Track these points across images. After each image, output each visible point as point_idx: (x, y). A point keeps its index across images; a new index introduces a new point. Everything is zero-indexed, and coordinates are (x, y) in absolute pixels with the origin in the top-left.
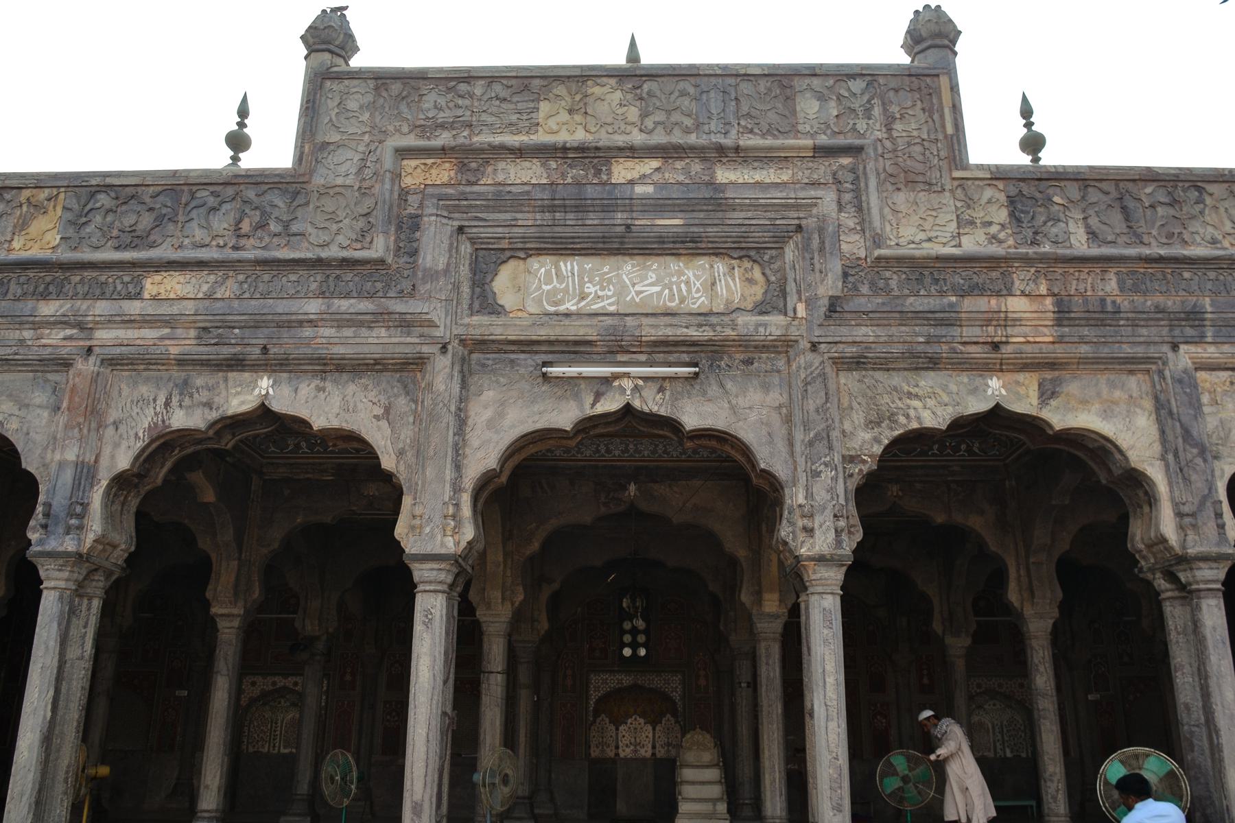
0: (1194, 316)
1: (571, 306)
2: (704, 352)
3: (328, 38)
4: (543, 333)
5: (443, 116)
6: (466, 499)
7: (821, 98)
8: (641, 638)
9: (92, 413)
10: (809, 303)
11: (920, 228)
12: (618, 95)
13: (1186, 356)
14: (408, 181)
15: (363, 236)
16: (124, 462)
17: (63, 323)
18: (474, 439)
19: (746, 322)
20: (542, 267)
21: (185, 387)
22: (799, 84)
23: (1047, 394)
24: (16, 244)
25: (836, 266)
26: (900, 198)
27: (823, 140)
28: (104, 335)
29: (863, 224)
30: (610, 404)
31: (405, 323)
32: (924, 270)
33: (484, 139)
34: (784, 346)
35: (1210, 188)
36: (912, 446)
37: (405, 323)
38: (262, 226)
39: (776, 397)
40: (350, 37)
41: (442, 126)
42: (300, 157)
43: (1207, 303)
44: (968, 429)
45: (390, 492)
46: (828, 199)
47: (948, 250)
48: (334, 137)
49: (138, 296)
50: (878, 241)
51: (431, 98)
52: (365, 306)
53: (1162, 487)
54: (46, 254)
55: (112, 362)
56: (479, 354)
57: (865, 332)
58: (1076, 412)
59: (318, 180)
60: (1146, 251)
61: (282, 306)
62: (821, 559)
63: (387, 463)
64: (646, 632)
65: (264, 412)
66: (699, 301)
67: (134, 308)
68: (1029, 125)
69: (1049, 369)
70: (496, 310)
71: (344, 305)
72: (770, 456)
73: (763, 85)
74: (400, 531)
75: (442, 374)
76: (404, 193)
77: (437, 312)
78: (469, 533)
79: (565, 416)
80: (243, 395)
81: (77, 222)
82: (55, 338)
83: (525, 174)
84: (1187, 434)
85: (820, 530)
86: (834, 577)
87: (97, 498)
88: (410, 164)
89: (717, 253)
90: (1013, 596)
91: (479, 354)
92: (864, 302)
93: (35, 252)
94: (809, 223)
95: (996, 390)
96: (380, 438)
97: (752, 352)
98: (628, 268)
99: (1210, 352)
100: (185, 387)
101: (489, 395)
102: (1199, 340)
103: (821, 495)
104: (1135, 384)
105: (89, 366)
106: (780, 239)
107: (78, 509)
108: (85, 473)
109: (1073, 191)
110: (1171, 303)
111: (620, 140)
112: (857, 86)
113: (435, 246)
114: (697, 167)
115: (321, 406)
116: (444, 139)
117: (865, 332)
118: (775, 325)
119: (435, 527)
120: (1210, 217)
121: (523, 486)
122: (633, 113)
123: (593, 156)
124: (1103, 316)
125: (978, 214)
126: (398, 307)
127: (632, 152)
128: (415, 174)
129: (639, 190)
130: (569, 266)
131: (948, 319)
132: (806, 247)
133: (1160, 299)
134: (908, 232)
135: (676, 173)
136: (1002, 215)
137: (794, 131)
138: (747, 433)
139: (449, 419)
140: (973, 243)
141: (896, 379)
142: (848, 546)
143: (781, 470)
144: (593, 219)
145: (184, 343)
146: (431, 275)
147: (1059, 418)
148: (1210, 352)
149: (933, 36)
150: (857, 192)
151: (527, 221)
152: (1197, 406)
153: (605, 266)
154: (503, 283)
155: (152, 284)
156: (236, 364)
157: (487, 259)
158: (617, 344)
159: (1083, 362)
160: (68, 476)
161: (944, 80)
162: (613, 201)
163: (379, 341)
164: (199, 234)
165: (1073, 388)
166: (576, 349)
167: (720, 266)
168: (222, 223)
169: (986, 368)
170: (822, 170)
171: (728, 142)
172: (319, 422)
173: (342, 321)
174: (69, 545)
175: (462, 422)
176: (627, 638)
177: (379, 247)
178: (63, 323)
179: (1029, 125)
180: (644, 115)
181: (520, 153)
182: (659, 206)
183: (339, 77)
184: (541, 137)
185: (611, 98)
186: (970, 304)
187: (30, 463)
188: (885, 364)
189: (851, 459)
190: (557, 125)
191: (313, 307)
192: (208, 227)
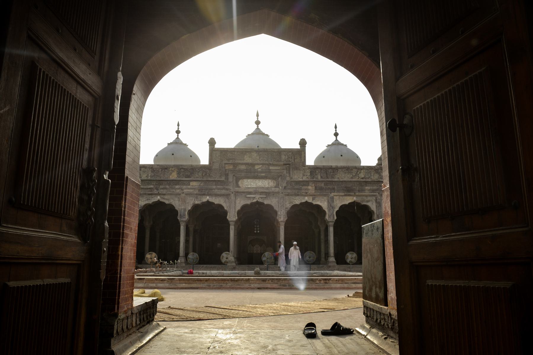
0: (334, 189)
2: (268, 194)
3: (212, 142)
4: (246, 191)
9: (184, 201)
11: (298, 176)
13: (332, 194)
15: (220, 177)
16: (190, 208)
17: (179, 189)
18: (237, 205)
19: (273, 189)
20: (245, 180)
21: (197, 198)
23: (313, 199)
26: (295, 171)
27: (285, 163)
28: (185, 191)
31: (227, 189)
32: (298, 183)
33: (237, 161)
34: (278, 193)
35: (340, 170)
37: (227, 189)
38: (206, 175)
39: (277, 200)
41: (231, 159)
43: (336, 187)
44: (302, 204)
45: (226, 213)
46: (285, 172)
47: (301, 180)
49: (189, 185)
50: (291, 178)
52: (221, 187)
53: (327, 212)
55: (186, 194)
56: (237, 193)
57: (289, 191)
59: (213, 168)
60: (328, 180)
61: (210, 187)
62: (281, 221)
63: (225, 208)
65: (208, 201)
66: (267, 186)
67: (189, 187)
69: (314, 197)
70: (239, 187)
71: (219, 187)
72: (276, 208)
74: (228, 217)
75: (232, 195)
76: (226, 170)
77: (231, 188)
78: (237, 218)
79: (249, 202)
80: (206, 199)
81: (179, 173)
82: (178, 191)
83: (243, 167)
85: (282, 217)
86: (283, 224)
87: (186, 213)
89: (270, 179)
91: (237, 193)
92: (288, 187)
95: (306, 199)
96: (224, 205)
97: (274, 194)
98: (257, 181)
99: (336, 194)
100: (197, 198)
102: (334, 192)
103: (282, 213)
104: (325, 198)
105: (184, 195)
106: (279, 177)
107: (184, 215)
108: (185, 210)
111: (256, 162)
112: (290, 153)
113: (231, 179)
115: (216, 201)
116: (230, 162)
119: (232, 217)
120: (338, 174)
121: (244, 211)
122: (258, 157)
123: (253, 165)
124: (321, 189)
125: (306, 174)
128: (228, 167)
130: (249, 180)
132: (282, 179)
136: (309, 174)
138: (273, 205)
140: (305, 178)
142: (285, 219)
143: (277, 210)
145: (197, 192)
147: (315, 203)
149: (303, 143)
150: (289, 170)
152: (333, 201)
154: (240, 183)
155: (191, 183)
156: (204, 195)
157: (237, 180)
158: (256, 193)
159: (318, 195)
160: (183, 211)
163: (223, 192)
164: (197, 176)
165: (317, 199)
166: (250, 193)
167: (270, 181)
168: (200, 174)
169: (305, 196)
170: (285, 167)
172: (216, 203)
173: (218, 189)
174: (184, 220)
176: (255, 229)
177: (223, 179)
178: (179, 189)
180: (260, 158)
181: (242, 164)
184: (245, 161)
185: (255, 155)
186: (303, 187)
187: (177, 208)
188: (292, 195)
190: (248, 159)
191: (214, 187)
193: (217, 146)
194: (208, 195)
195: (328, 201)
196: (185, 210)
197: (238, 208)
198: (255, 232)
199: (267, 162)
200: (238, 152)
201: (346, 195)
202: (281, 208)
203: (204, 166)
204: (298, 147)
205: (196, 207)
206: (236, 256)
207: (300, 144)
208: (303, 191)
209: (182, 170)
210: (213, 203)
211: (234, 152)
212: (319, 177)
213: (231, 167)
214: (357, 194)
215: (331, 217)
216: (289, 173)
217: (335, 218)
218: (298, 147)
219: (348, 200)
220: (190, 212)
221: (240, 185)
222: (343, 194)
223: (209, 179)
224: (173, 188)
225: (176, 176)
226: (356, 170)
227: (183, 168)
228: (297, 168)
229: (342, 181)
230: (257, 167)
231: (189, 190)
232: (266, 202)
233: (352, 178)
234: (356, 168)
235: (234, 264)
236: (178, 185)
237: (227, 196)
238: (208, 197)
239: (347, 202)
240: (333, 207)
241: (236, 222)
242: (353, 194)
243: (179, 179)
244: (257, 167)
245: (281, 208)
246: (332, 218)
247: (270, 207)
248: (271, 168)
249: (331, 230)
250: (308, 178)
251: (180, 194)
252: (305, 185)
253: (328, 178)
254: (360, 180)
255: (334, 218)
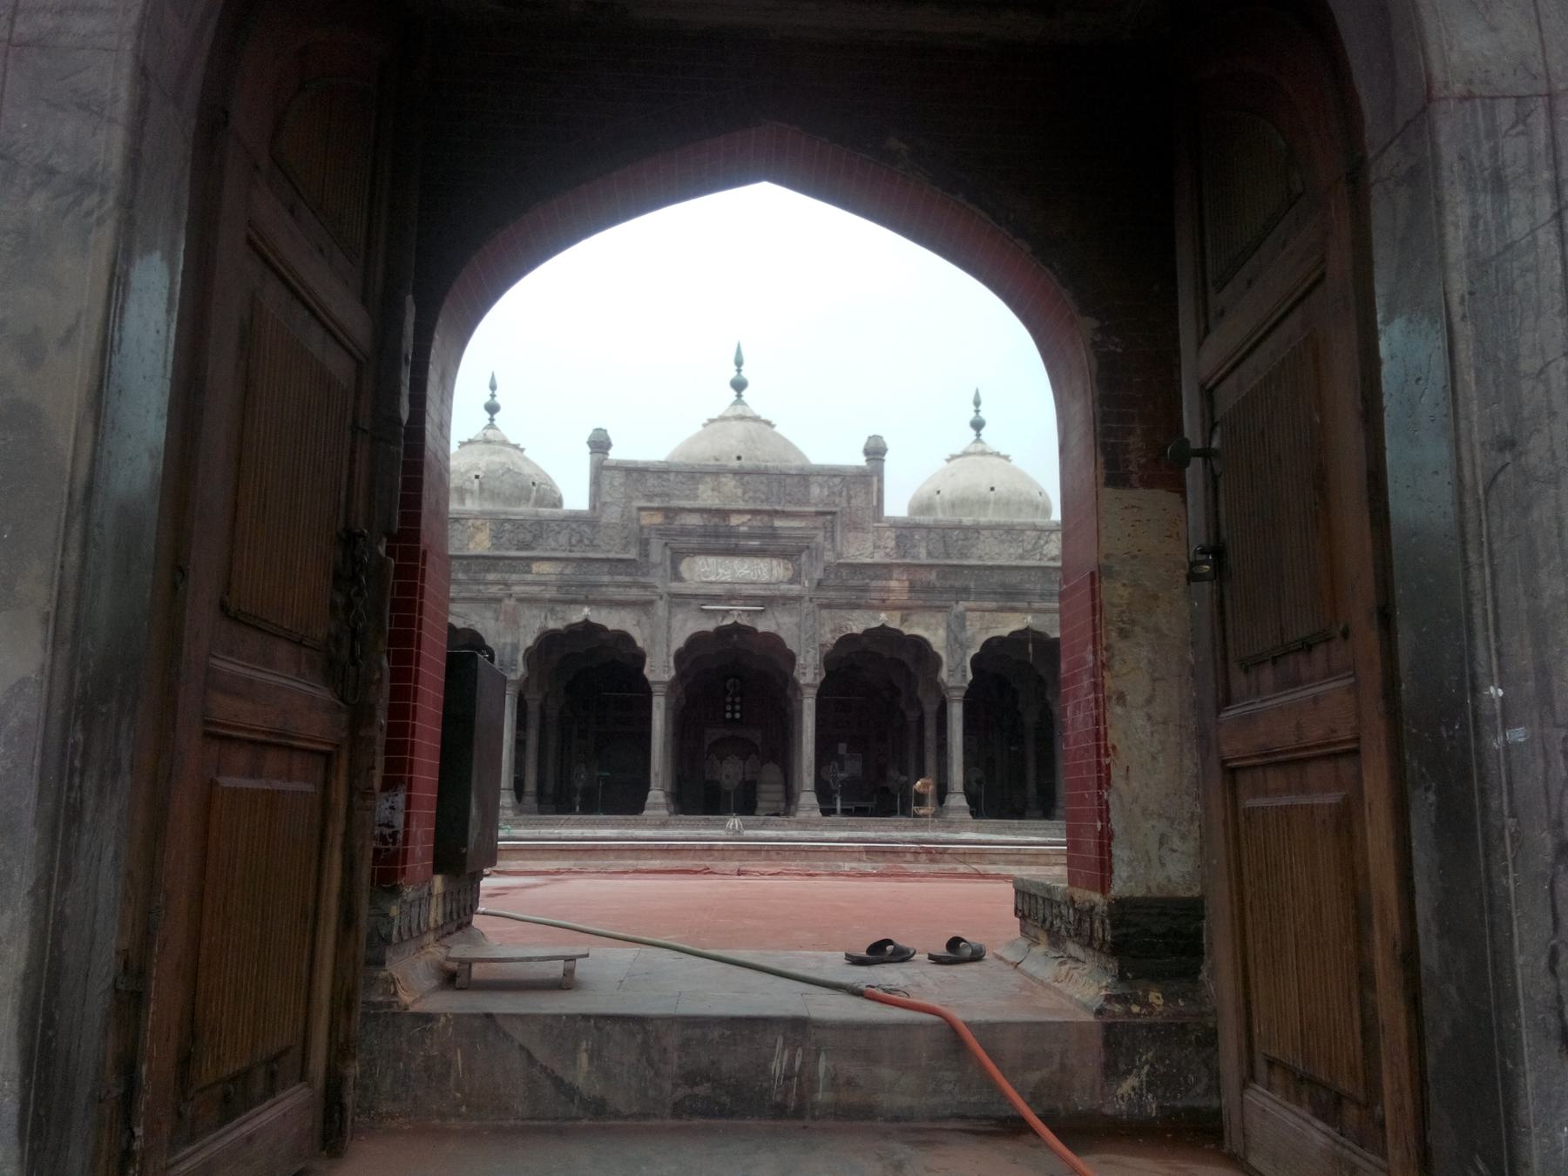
1: (712, 578)
2: (768, 602)
3: (599, 444)
5: (657, 490)
6: (672, 660)
7: (821, 486)
8: (738, 707)
9: (513, 621)
10: (810, 581)
11: (860, 550)
12: (733, 483)
13: (962, 606)
14: (643, 522)
15: (625, 548)
19: (783, 587)
21: (552, 610)
22: (812, 479)
23: (903, 620)
24: (471, 546)
25: (821, 566)
26: (851, 535)
27: (821, 508)
28: (516, 589)
29: (833, 549)
30: (728, 621)
31: (645, 586)
32: (857, 568)
33: (675, 503)
34: (798, 599)
35: (985, 533)
36: (848, 640)
37: (645, 586)
39: (795, 619)
40: (608, 439)
42: (593, 507)
43: (972, 585)
44: (868, 633)
45: (639, 658)
46: (821, 534)
47: (869, 561)
48: (609, 499)
49: (530, 572)
50: (839, 556)
51: (651, 481)
52: (628, 579)
53: (944, 659)
54: (486, 553)
55: (520, 600)
57: (832, 594)
58: (916, 628)
60: (949, 562)
61: (592, 578)
62: (808, 685)
63: (640, 644)
64: (741, 704)
66: (765, 578)
67: (529, 577)
68: (977, 411)
69: (906, 610)
72: (791, 644)
73: (796, 479)
74: (646, 671)
75: (661, 608)
76: (642, 528)
77: (657, 581)
78: (673, 673)
79: (709, 626)
80: (579, 615)
81: (496, 536)
82: (494, 590)
83: (693, 520)
84: (956, 639)
85: (809, 673)
87: (520, 658)
88: (643, 513)
89: (773, 555)
90: (919, 693)
92: (830, 582)
93: (479, 551)
94: (812, 545)
96: (635, 633)
97: (786, 601)
99: (972, 604)
101: (680, 616)
102: (967, 600)
103: (810, 660)
104: (940, 617)
105: (512, 602)
106: (800, 551)
107: (514, 662)
108: (515, 647)
109: (924, 533)
110: (957, 584)
111: (734, 506)
112: (837, 480)
113: (657, 552)
114: (766, 519)
115: (612, 620)
116: (655, 505)
117: (832, 594)
118: (795, 589)
119: (659, 670)
120: (981, 546)
122: (739, 492)
123: (724, 513)
124: (928, 589)
125: (882, 544)
126: (642, 580)
127: (739, 512)
128: (647, 519)
129: (743, 529)
130: (712, 560)
131: (865, 589)
132: (810, 556)
133: (951, 582)
134: (852, 551)
135: (757, 522)
136: (892, 544)
137: (808, 503)
139: (664, 627)
140: (879, 558)
141: (843, 613)
142: (818, 681)
143: (795, 651)
144: (722, 541)
145: (551, 593)
146: (655, 566)
147: (907, 631)
148: (972, 604)
149: (876, 451)
151: (694, 542)
152: (963, 627)
153: (727, 561)
154: (684, 567)
155: (536, 567)
156: (574, 602)
157: (677, 556)
158: (731, 597)
160: (508, 649)
161: (875, 479)
162: (731, 533)
163: (634, 594)
164: (553, 544)
165: (914, 618)
166: (715, 598)
167: (775, 562)
168: (563, 539)
170: (820, 521)
171: (778, 508)
172: (610, 627)
173: (618, 585)
175: (669, 628)
176: (729, 708)
177: (632, 554)
179: (977, 411)
181: (691, 511)
182: (750, 536)
183: (609, 468)
185: (730, 483)
186: (874, 584)
188: (840, 607)
189: (822, 645)
190: (707, 497)
191: (606, 579)
192: (556, 541)
193: (615, 455)
194: (588, 602)
195: (949, 626)
196: (515, 647)
197: (679, 642)
198: (728, 715)
199: (766, 507)
200: (678, 473)
201: (1001, 610)
202: (807, 642)
203: (575, 518)
204: (860, 460)
205: (549, 641)
206: (668, 789)
207: (866, 452)
208: (874, 595)
209: (508, 526)
210: (603, 629)
211: (667, 472)
212: (923, 552)
213: (658, 519)
214: (1036, 605)
215: (955, 675)
216: (833, 540)
217: (970, 677)
218: (860, 460)
219: (1009, 625)
220: (533, 656)
221: (686, 575)
222: (993, 605)
223: (591, 555)
224: (477, 582)
225: (487, 544)
226: (1034, 533)
227: (509, 520)
228: (856, 526)
229: (991, 568)
230: (735, 520)
231: (528, 588)
232: (763, 626)
233: (1021, 557)
234: (1034, 528)
235: (665, 812)
236: (495, 571)
237: (645, 605)
238: (586, 610)
239: (1005, 631)
240: (961, 645)
241: (672, 685)
242: (1024, 605)
243: (497, 553)
244: (735, 520)
245: (807, 642)
246: (959, 676)
247: (773, 640)
248: (778, 523)
249: (956, 712)
250: (887, 555)
251: (499, 600)
252: (877, 577)
253: (948, 556)
254: (1045, 563)
255: (964, 676)
